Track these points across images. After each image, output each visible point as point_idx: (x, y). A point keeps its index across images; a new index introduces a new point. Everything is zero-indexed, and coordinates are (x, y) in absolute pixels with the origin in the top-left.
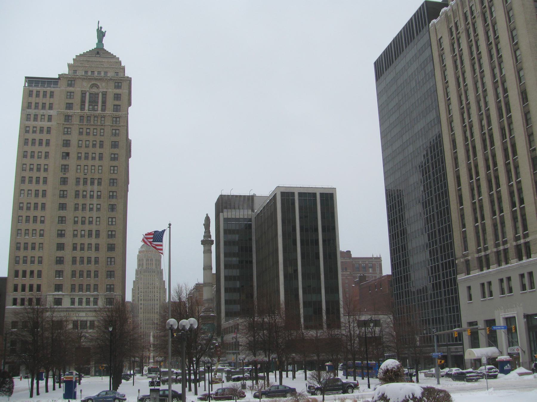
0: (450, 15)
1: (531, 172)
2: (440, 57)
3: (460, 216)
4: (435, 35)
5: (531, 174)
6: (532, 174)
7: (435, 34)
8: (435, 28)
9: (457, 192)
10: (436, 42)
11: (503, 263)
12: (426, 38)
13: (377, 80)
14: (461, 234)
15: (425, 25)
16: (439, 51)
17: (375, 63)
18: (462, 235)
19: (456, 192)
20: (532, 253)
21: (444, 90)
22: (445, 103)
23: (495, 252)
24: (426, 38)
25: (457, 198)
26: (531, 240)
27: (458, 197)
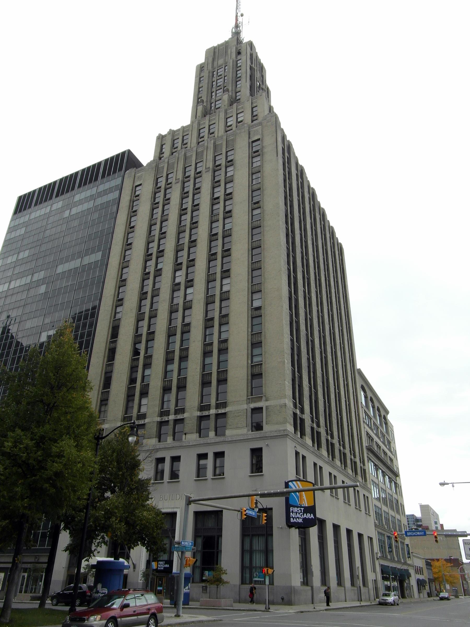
0: (163, 168)
1: (248, 331)
2: (132, 202)
3: (104, 372)
4: (132, 182)
5: (248, 333)
6: (250, 334)
7: (133, 180)
8: (135, 175)
9: (108, 343)
10: (131, 187)
11: (170, 439)
12: (118, 181)
13: (15, 212)
14: (98, 395)
15: (120, 169)
16: (131, 196)
17: (20, 198)
18: (100, 396)
19: (106, 344)
20: (228, 426)
21: (125, 233)
22: (123, 247)
23: (157, 421)
24: (118, 181)
25: (105, 351)
26: (231, 411)
27: (107, 350)
